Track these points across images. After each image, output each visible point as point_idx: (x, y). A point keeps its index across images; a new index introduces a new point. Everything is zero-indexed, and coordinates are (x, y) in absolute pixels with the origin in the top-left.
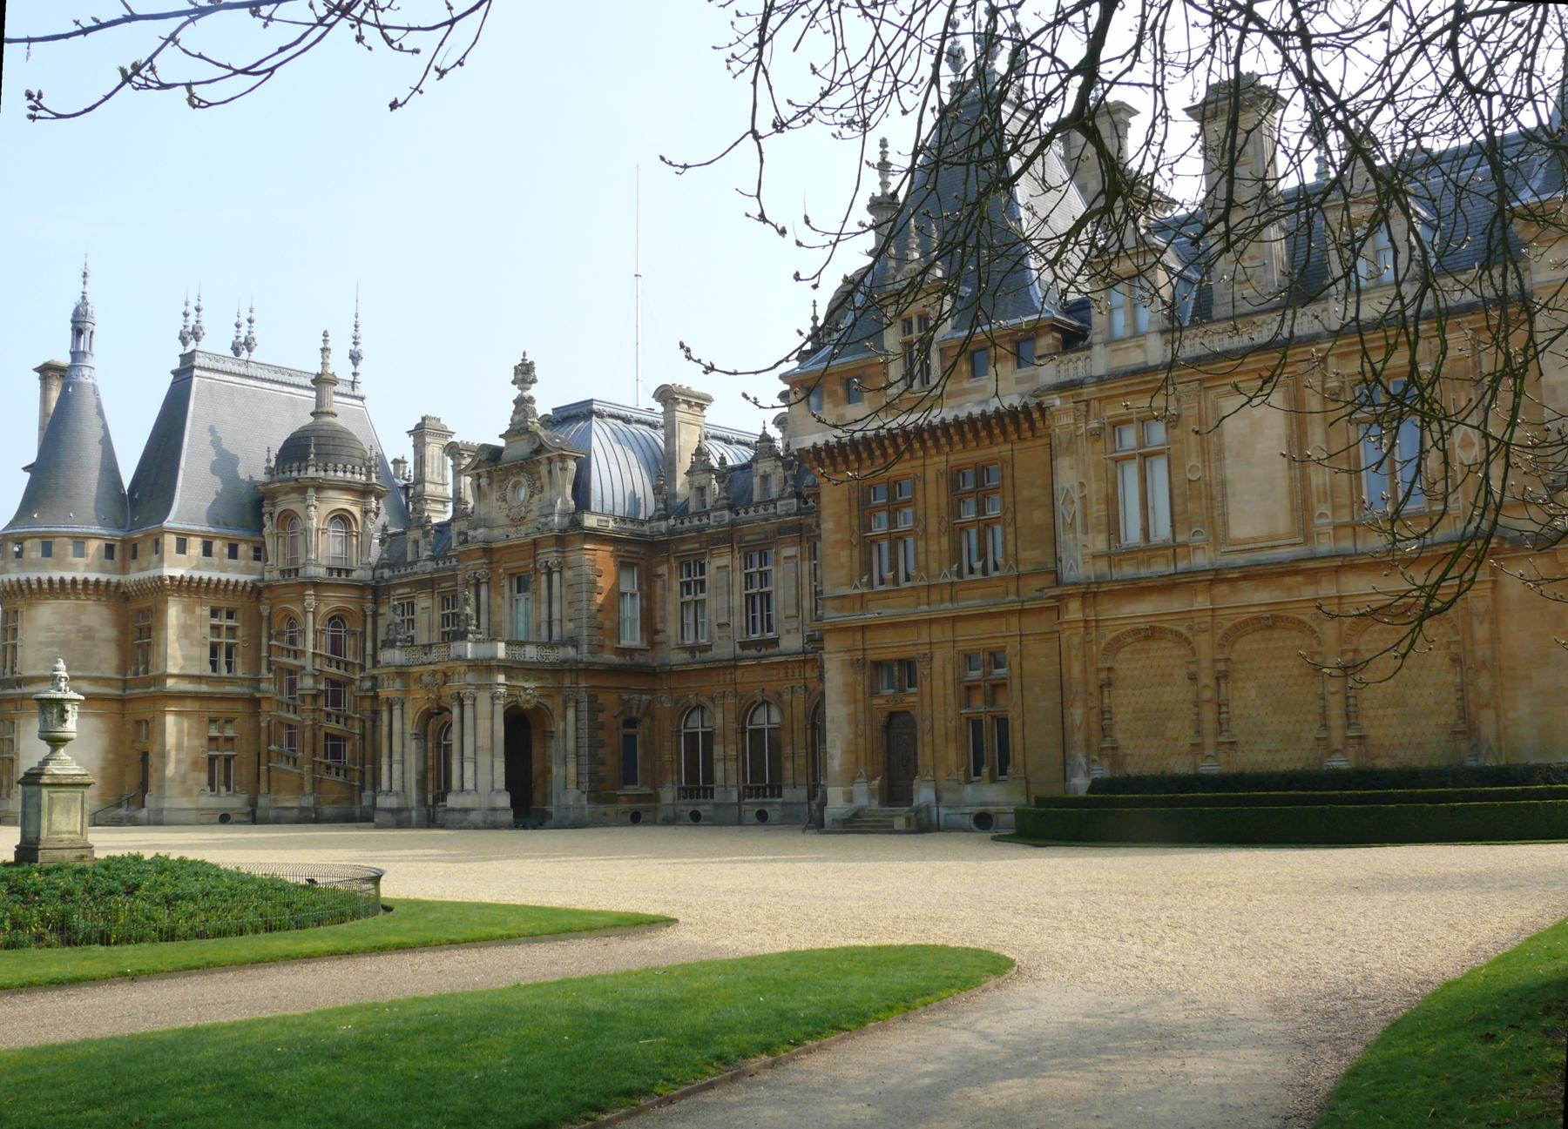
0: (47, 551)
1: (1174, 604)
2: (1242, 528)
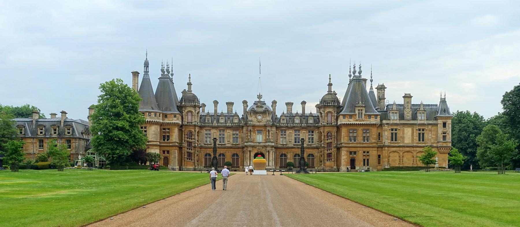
0: (155, 116)
1: (398, 149)
2: (405, 142)
